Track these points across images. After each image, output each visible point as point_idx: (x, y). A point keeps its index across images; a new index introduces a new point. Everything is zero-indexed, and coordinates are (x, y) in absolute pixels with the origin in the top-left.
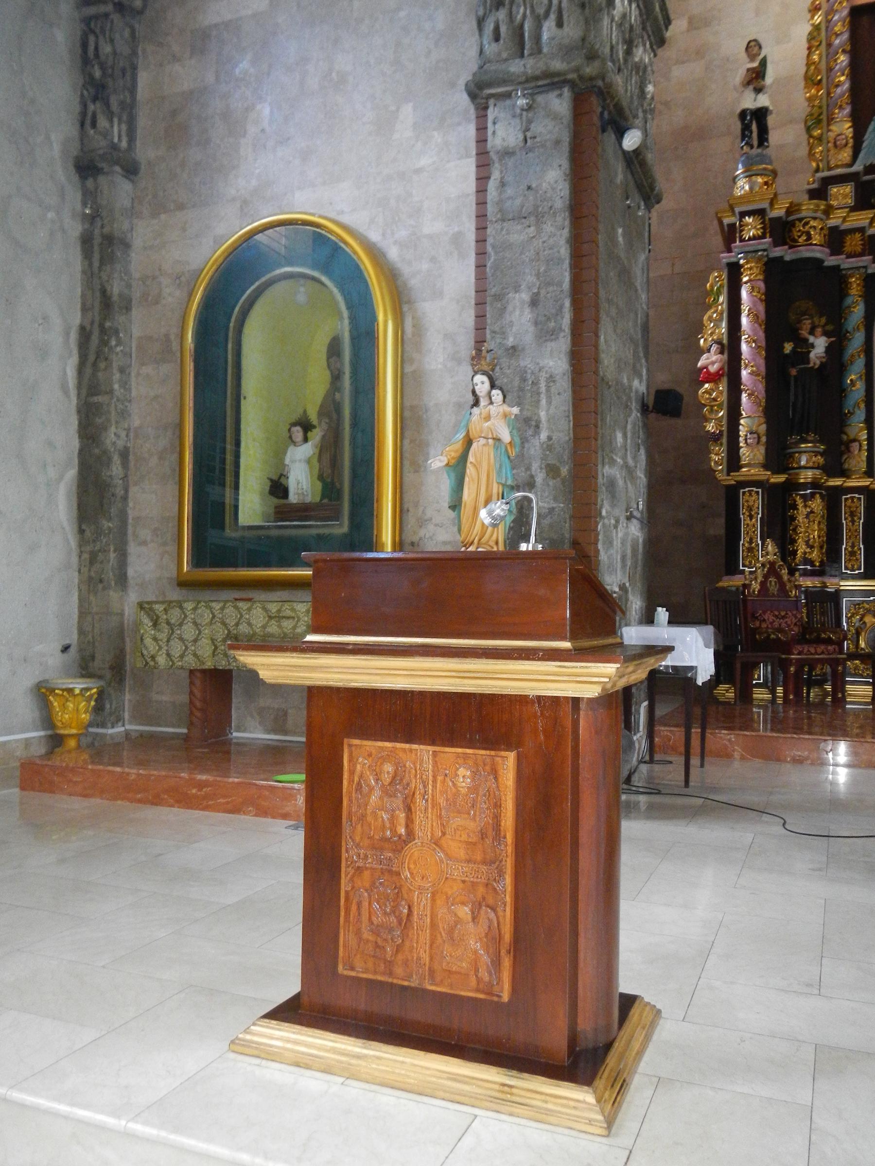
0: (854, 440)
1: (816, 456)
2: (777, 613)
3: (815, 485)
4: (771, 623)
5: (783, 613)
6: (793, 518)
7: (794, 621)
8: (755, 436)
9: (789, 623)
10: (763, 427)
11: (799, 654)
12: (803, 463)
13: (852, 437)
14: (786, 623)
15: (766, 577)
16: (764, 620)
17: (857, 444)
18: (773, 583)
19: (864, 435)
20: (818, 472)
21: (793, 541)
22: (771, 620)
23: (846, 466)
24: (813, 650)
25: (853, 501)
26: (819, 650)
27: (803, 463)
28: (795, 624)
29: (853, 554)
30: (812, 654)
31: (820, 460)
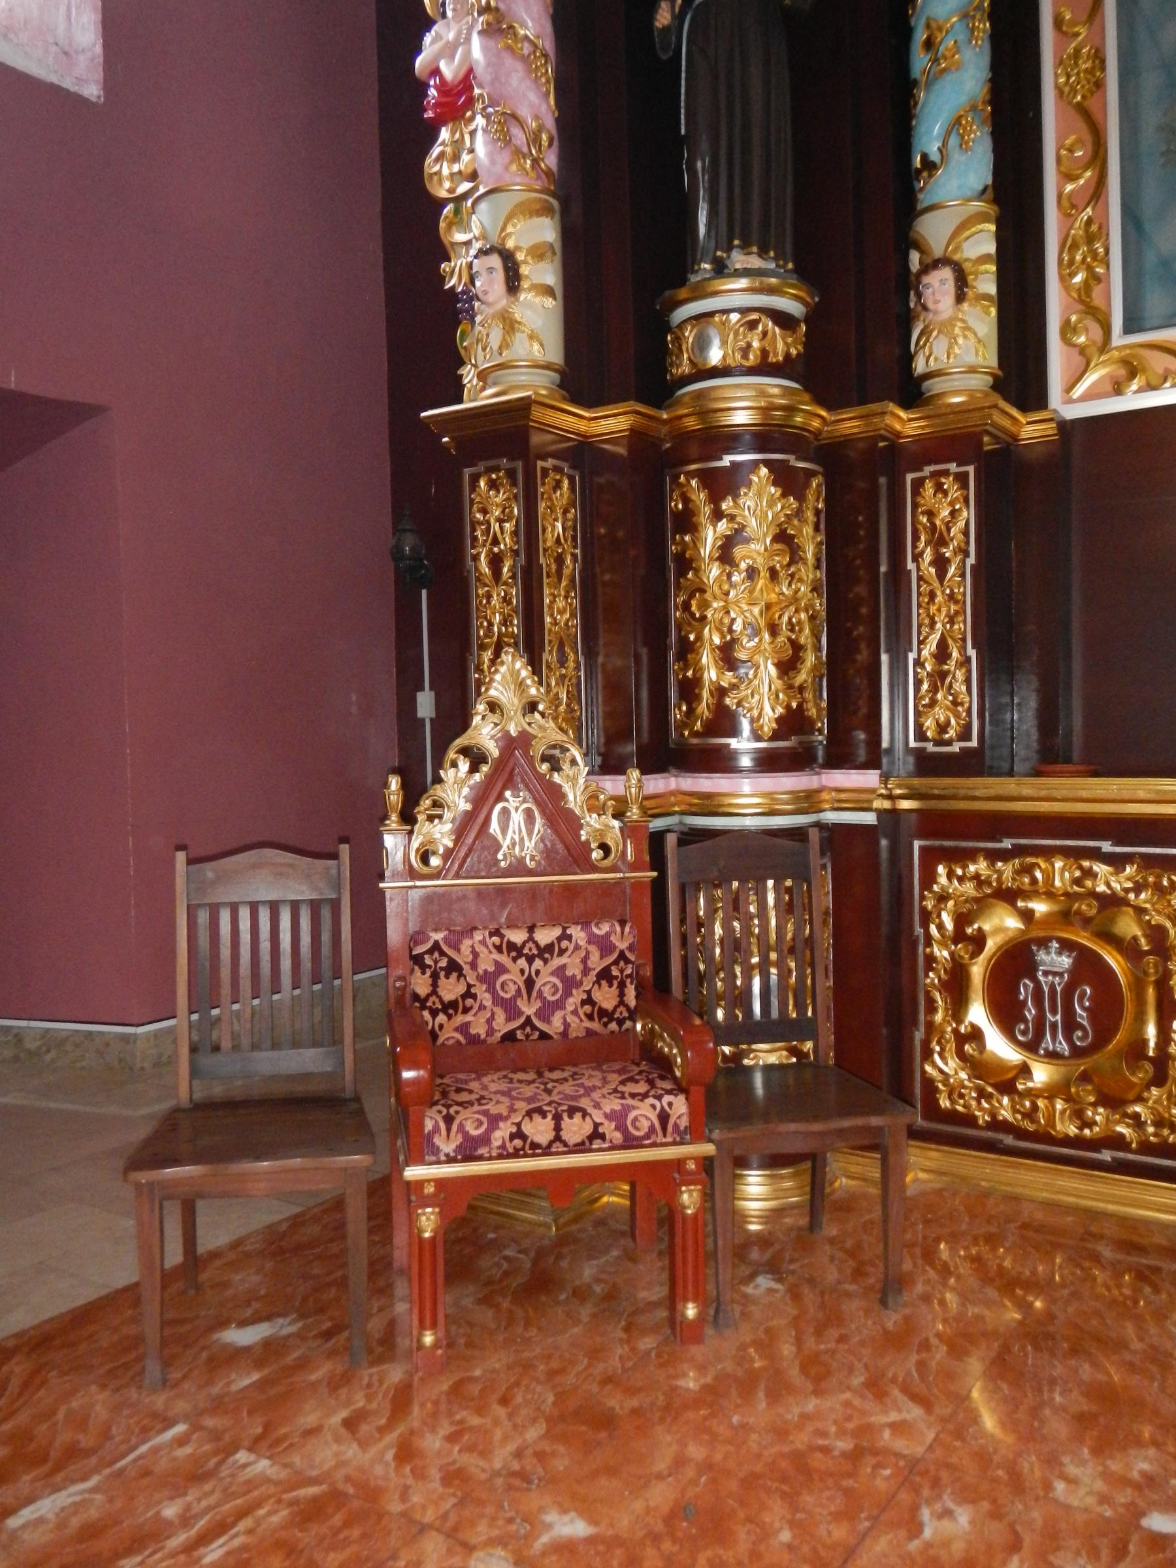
0: (944, 261)
1: (752, 325)
2: (517, 937)
3: (764, 438)
4: (488, 979)
5: (545, 936)
6: (686, 563)
7: (597, 962)
8: (495, 261)
9: (574, 970)
10: (546, 231)
11: (468, 1152)
12: (715, 356)
13: (938, 251)
14: (560, 971)
15: (483, 798)
16: (454, 967)
17: (946, 274)
18: (517, 818)
19: (982, 244)
20: (774, 385)
21: (687, 650)
22: (486, 964)
23: (920, 366)
24: (540, 1130)
25: (939, 488)
26: (575, 1129)
27: (715, 356)
28: (605, 975)
29: (939, 677)
30: (537, 1149)
31: (782, 345)
